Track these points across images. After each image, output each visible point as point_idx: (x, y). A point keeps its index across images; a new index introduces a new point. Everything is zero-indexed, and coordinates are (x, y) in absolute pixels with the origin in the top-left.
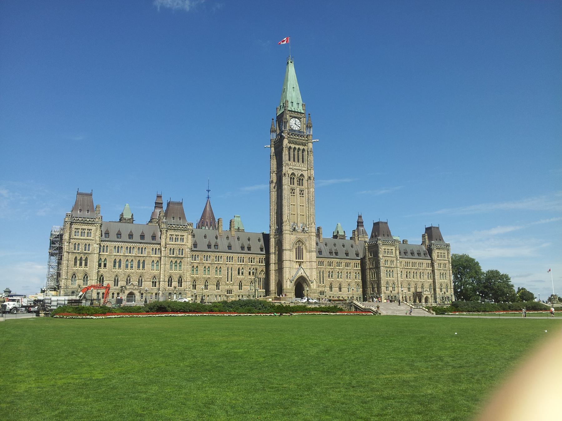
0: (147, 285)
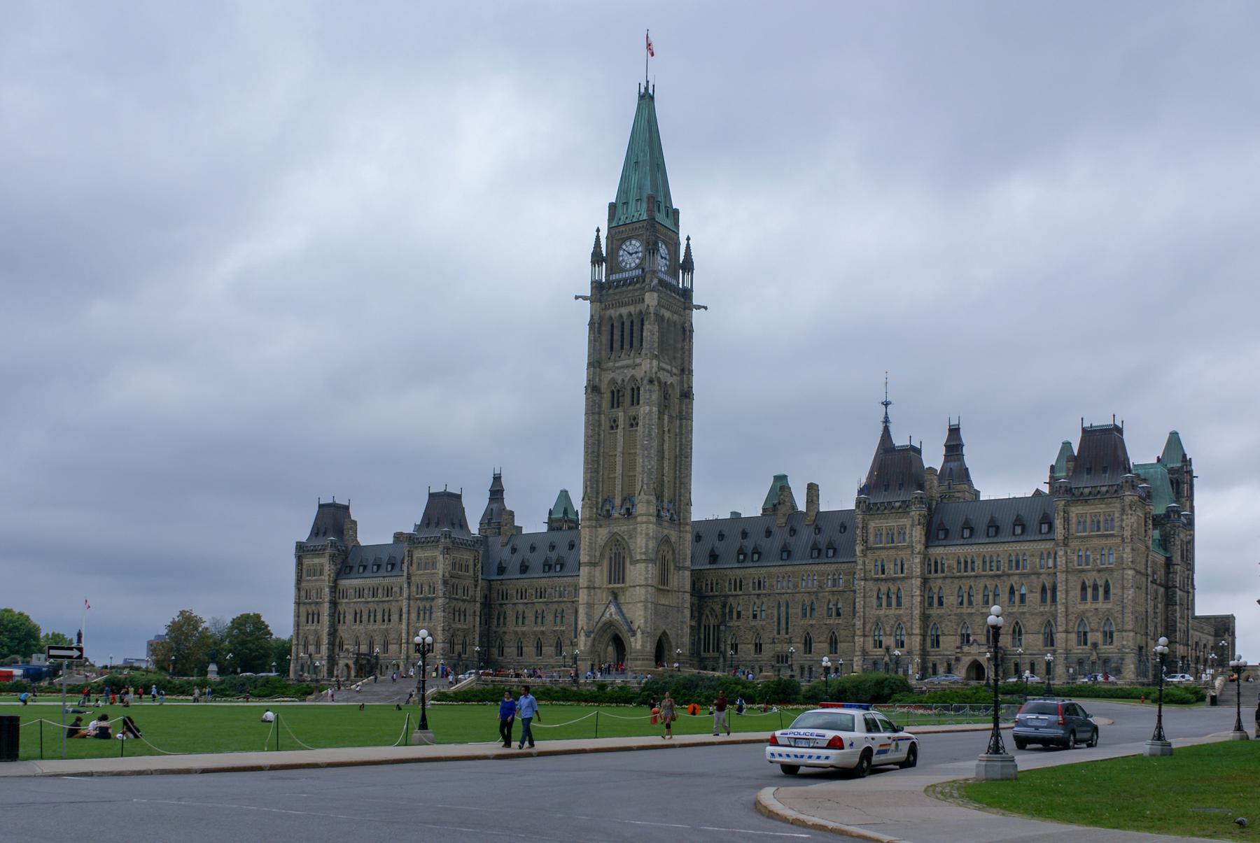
0: (393, 648)
